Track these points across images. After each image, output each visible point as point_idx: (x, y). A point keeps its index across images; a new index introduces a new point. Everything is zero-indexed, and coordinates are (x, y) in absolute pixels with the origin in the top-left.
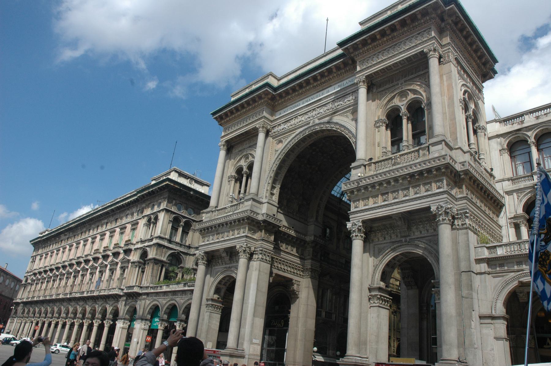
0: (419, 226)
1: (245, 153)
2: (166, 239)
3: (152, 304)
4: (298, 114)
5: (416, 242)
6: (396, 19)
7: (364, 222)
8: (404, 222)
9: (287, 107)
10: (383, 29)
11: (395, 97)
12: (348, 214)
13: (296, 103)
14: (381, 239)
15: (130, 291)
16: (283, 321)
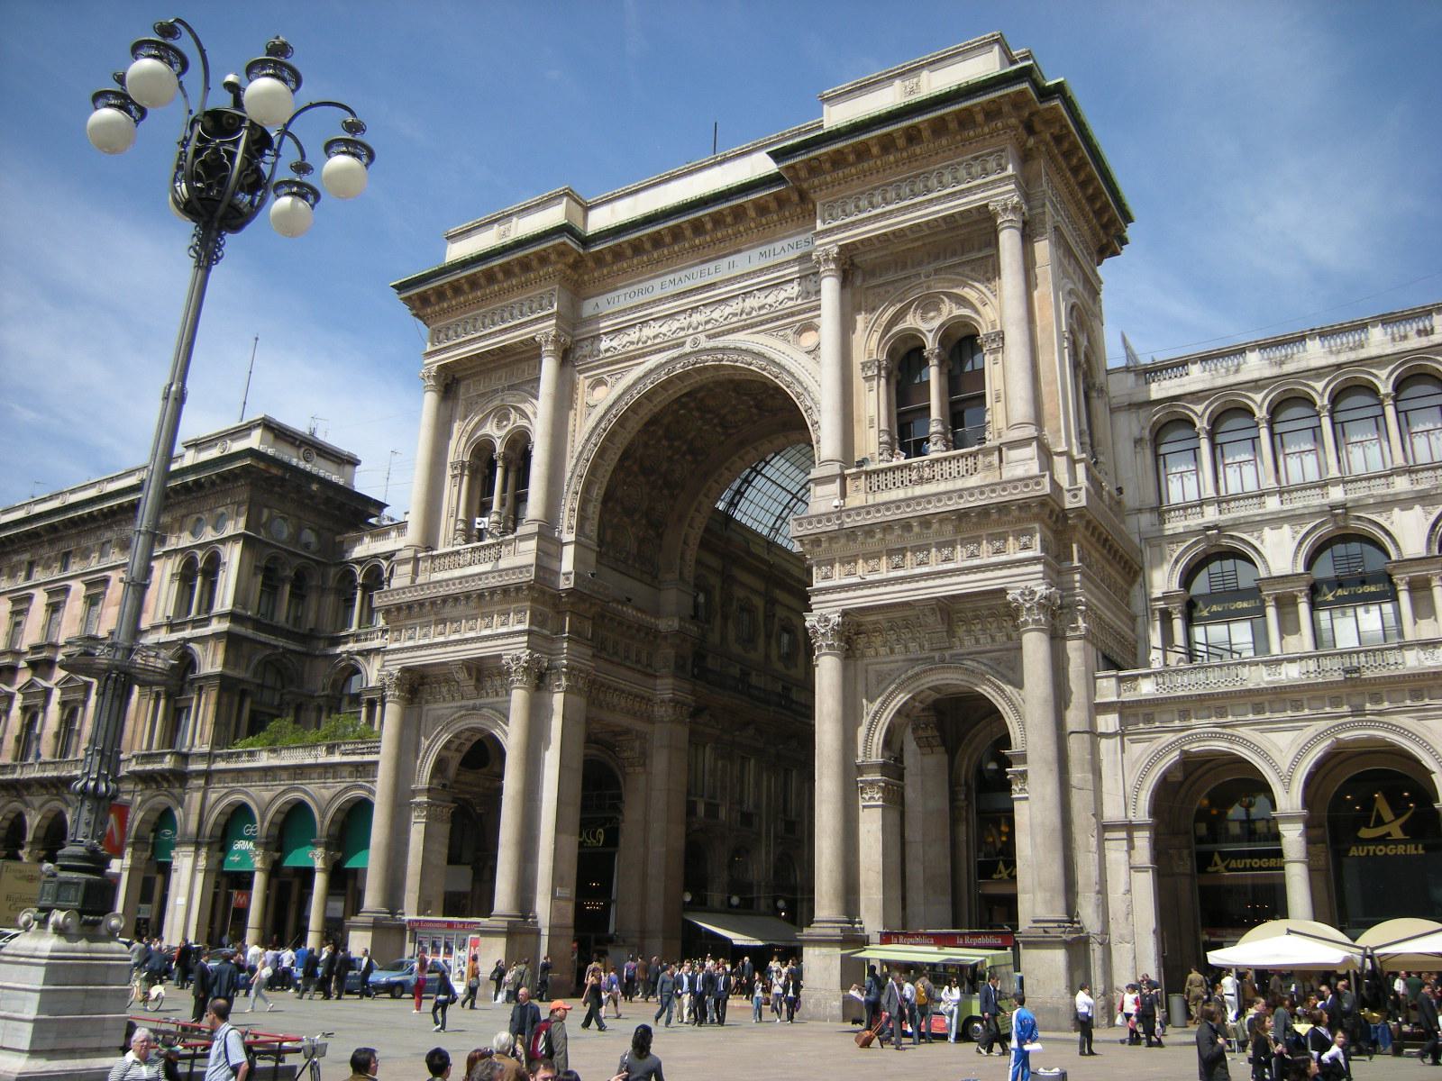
0: (973, 628)
1: (497, 402)
2: (249, 618)
3: (226, 802)
4: (651, 314)
5: (965, 662)
6: (921, 115)
7: (845, 614)
8: (942, 619)
9: (616, 289)
10: (889, 134)
11: (910, 307)
12: (807, 592)
13: (640, 282)
14: (882, 651)
15: (149, 767)
16: (601, 830)
